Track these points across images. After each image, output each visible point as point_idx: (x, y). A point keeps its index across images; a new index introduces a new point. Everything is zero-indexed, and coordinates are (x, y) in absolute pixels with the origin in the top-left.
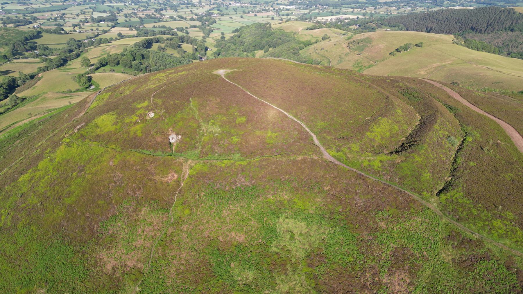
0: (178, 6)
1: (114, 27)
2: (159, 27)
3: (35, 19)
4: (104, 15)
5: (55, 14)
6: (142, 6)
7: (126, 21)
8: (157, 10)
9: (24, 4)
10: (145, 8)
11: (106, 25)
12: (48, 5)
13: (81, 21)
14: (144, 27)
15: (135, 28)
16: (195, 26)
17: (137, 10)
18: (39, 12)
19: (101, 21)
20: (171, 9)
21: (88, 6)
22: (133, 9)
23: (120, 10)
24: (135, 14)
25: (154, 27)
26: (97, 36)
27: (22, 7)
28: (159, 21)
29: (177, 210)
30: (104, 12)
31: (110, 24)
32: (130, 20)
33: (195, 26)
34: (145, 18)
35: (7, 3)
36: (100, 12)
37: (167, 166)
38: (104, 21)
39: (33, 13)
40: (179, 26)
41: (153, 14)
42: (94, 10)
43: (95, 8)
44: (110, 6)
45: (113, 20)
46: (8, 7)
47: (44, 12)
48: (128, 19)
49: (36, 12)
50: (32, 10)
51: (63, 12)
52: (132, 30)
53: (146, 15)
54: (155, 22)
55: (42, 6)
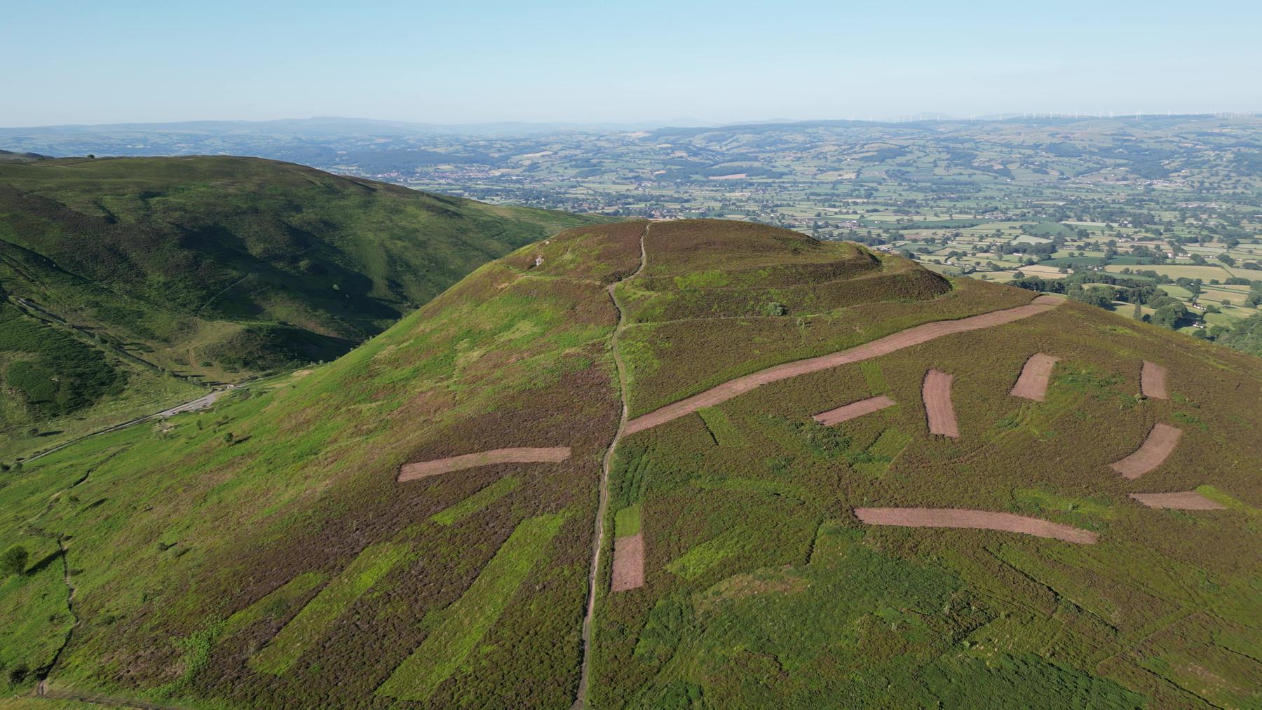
0: (1246, 236)
1: (1031, 263)
2: (1139, 273)
3: (902, 237)
4: (1033, 241)
5: (941, 232)
6: (1147, 231)
7: (1072, 255)
8: (1180, 240)
9: (907, 213)
10: (1149, 235)
11: (1016, 260)
12: (945, 217)
13: (975, 247)
14: (1103, 270)
15: (1077, 269)
16: (1243, 282)
17: (1128, 236)
18: (919, 227)
19: (1017, 251)
20: (1221, 241)
21: (1017, 224)
22: (1119, 235)
23: (1083, 234)
24: (1112, 243)
25: (1126, 271)
26: (970, 272)
27: (893, 218)
28: (1153, 263)
29: (484, 306)
30: (1046, 236)
31: (1026, 257)
32: (1082, 254)
33: (1243, 282)
34: (1127, 253)
35: (876, 211)
36: (1036, 235)
37: (510, 277)
38: (1024, 252)
39: (905, 228)
40: (1195, 277)
41: (1158, 247)
42: (1025, 232)
43: (1031, 226)
44: (1069, 226)
45: (1045, 254)
46: (875, 217)
47: (927, 228)
48: (1077, 253)
49: (911, 228)
50: (906, 224)
51: (961, 230)
52: (1066, 272)
53: (1139, 248)
54: (1139, 263)
55: (931, 218)
